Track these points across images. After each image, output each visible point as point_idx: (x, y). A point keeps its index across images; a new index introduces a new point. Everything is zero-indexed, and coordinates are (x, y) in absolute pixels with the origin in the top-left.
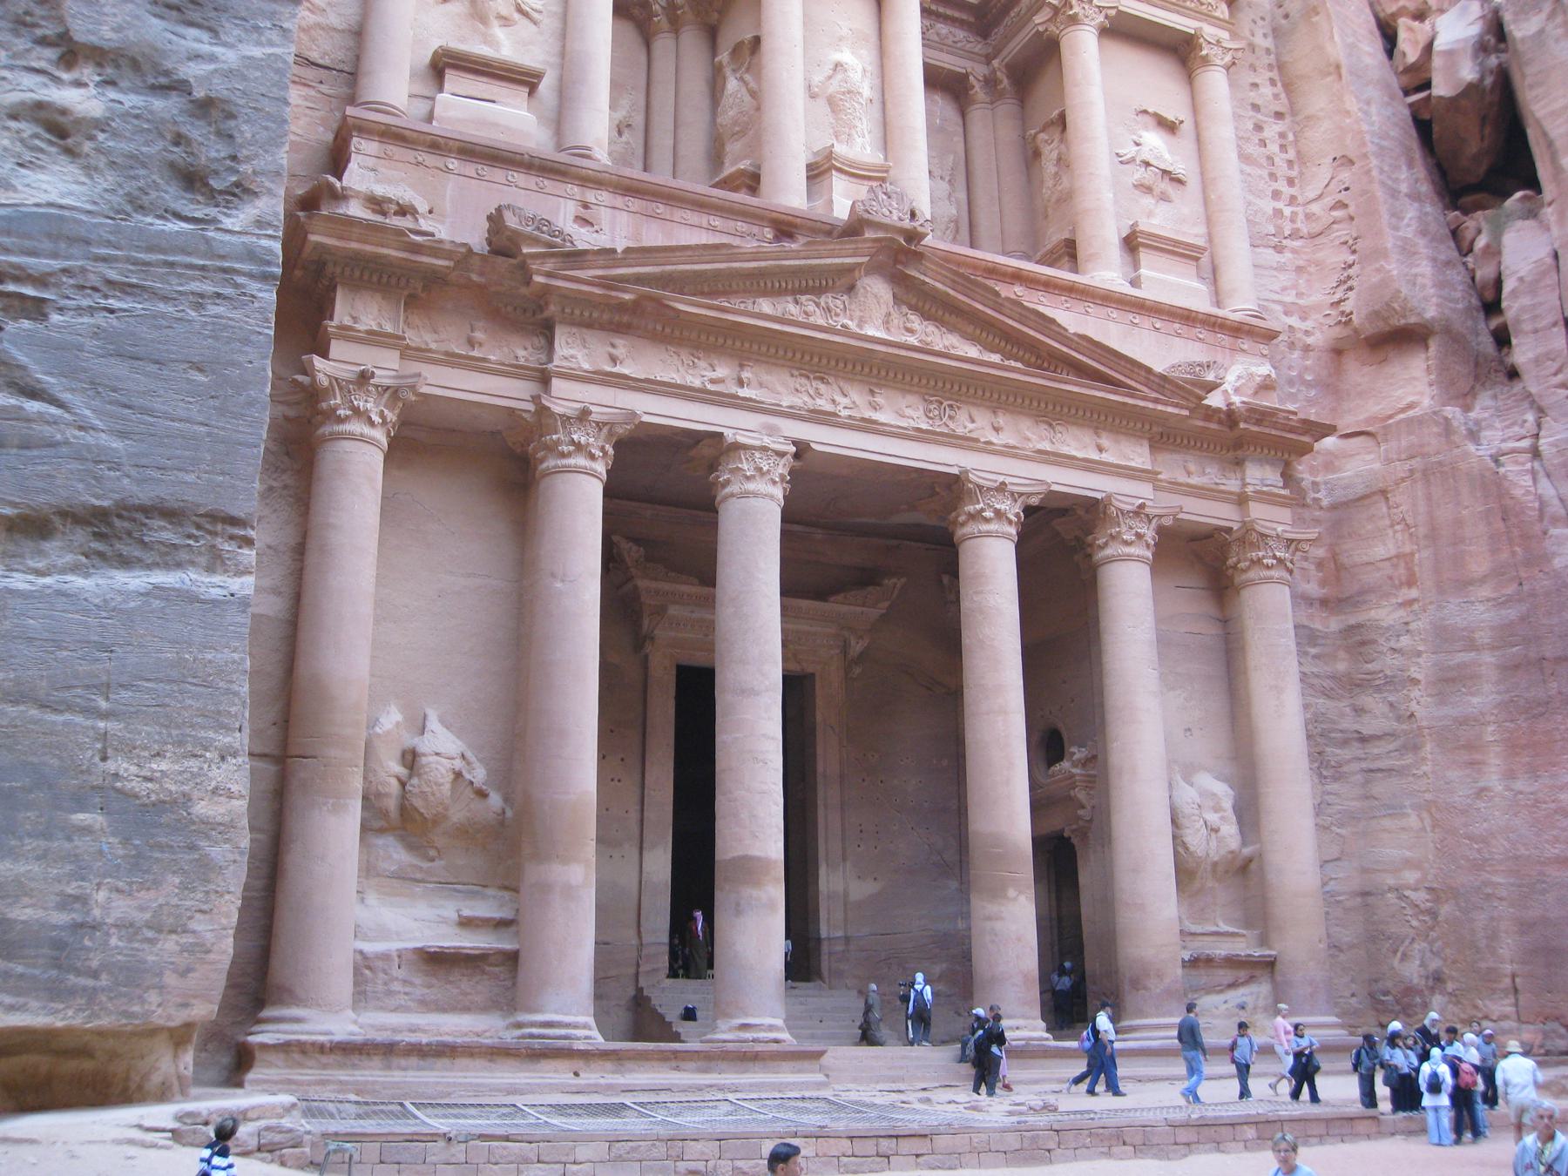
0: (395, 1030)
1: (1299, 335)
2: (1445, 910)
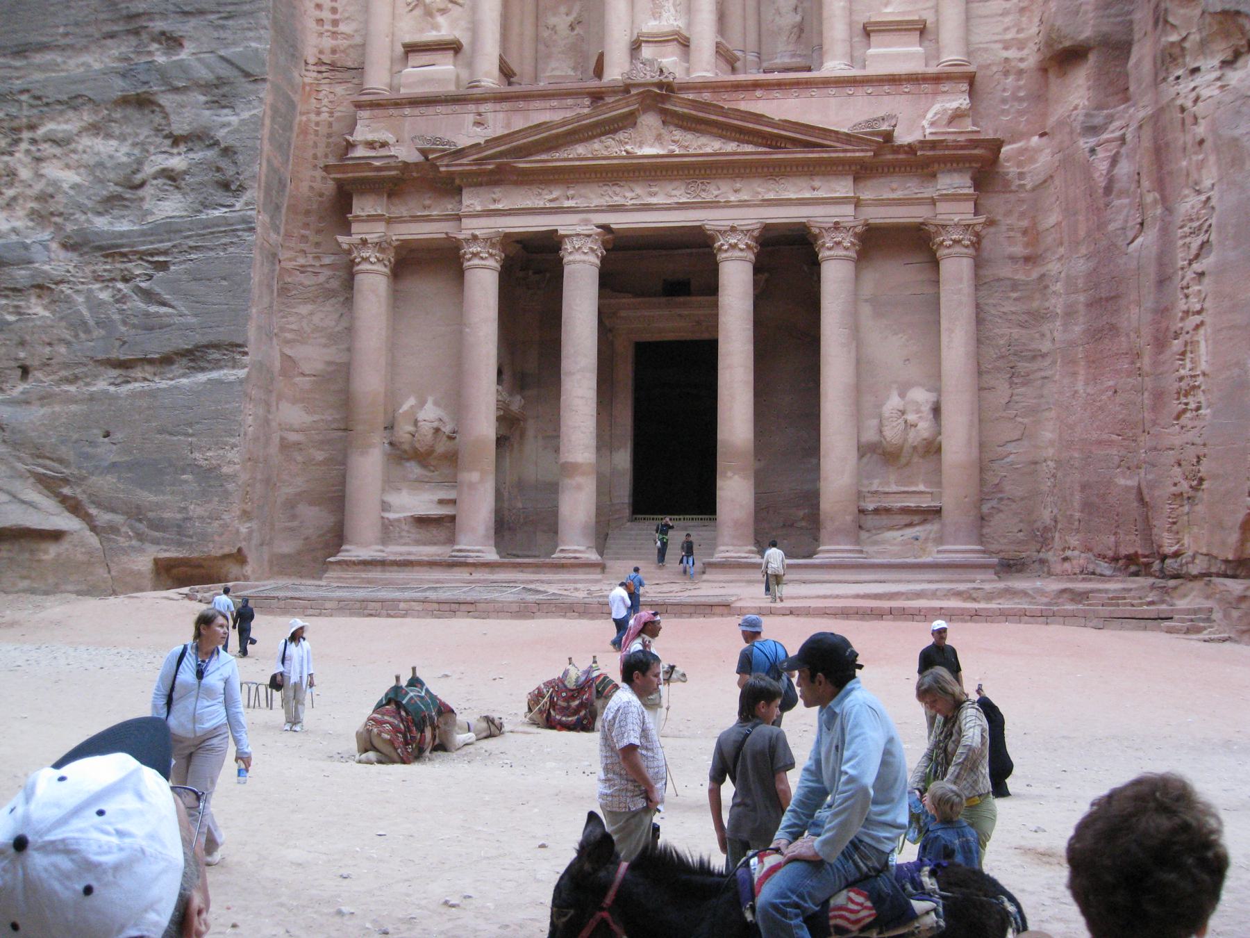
0: (401, 554)
1: (1013, 64)
2: (1059, 474)
